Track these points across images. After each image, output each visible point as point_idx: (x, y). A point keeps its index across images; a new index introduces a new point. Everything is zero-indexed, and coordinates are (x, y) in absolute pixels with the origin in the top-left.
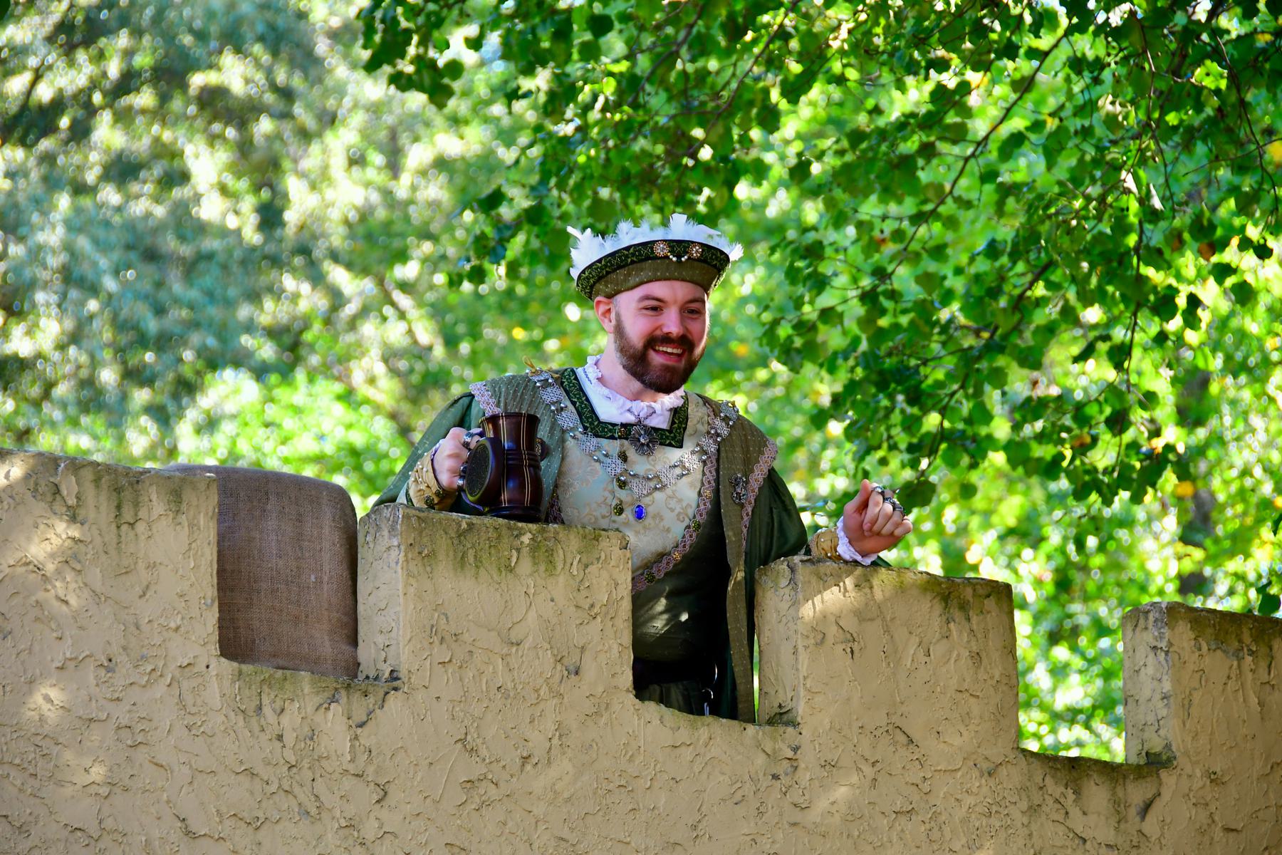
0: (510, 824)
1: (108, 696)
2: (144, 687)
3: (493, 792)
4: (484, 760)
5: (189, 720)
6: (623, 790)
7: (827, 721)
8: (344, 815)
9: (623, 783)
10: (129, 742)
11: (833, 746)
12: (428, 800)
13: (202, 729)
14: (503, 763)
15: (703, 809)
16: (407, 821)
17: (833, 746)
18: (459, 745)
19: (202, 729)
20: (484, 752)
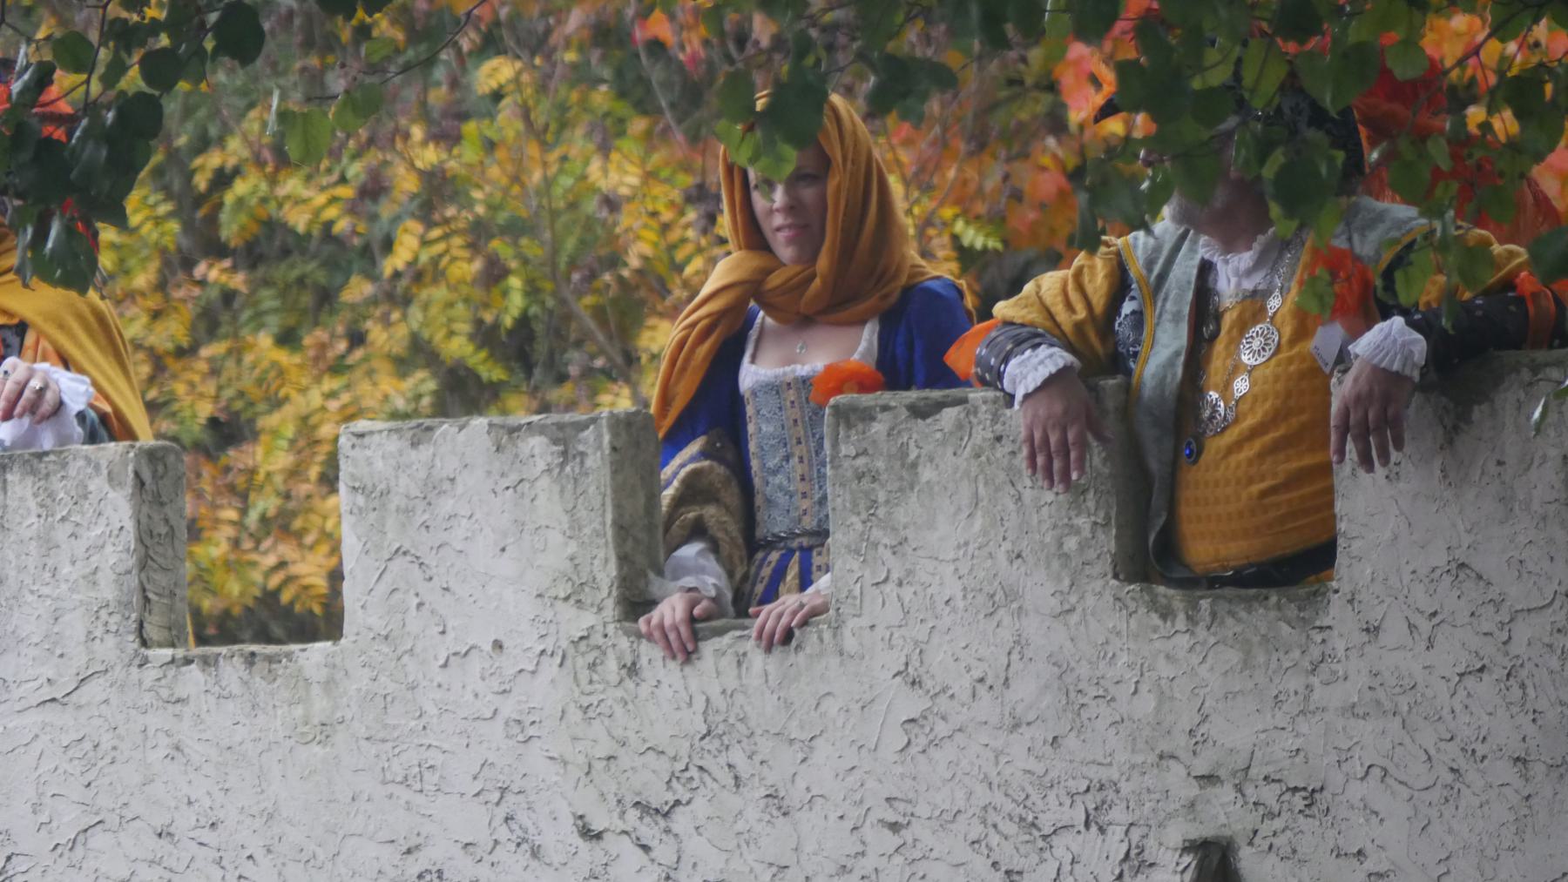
0: (964, 763)
1: (496, 689)
2: (533, 672)
3: (942, 729)
4: (928, 691)
5: (585, 701)
6: (1100, 701)
7: (1369, 571)
8: (764, 782)
9: (1101, 693)
10: (521, 738)
11: (1376, 602)
12: (864, 751)
13: (598, 710)
14: (950, 692)
15: (1206, 710)
16: (841, 777)
17: (1376, 602)
18: (898, 679)
19: (598, 710)
20: (928, 683)
